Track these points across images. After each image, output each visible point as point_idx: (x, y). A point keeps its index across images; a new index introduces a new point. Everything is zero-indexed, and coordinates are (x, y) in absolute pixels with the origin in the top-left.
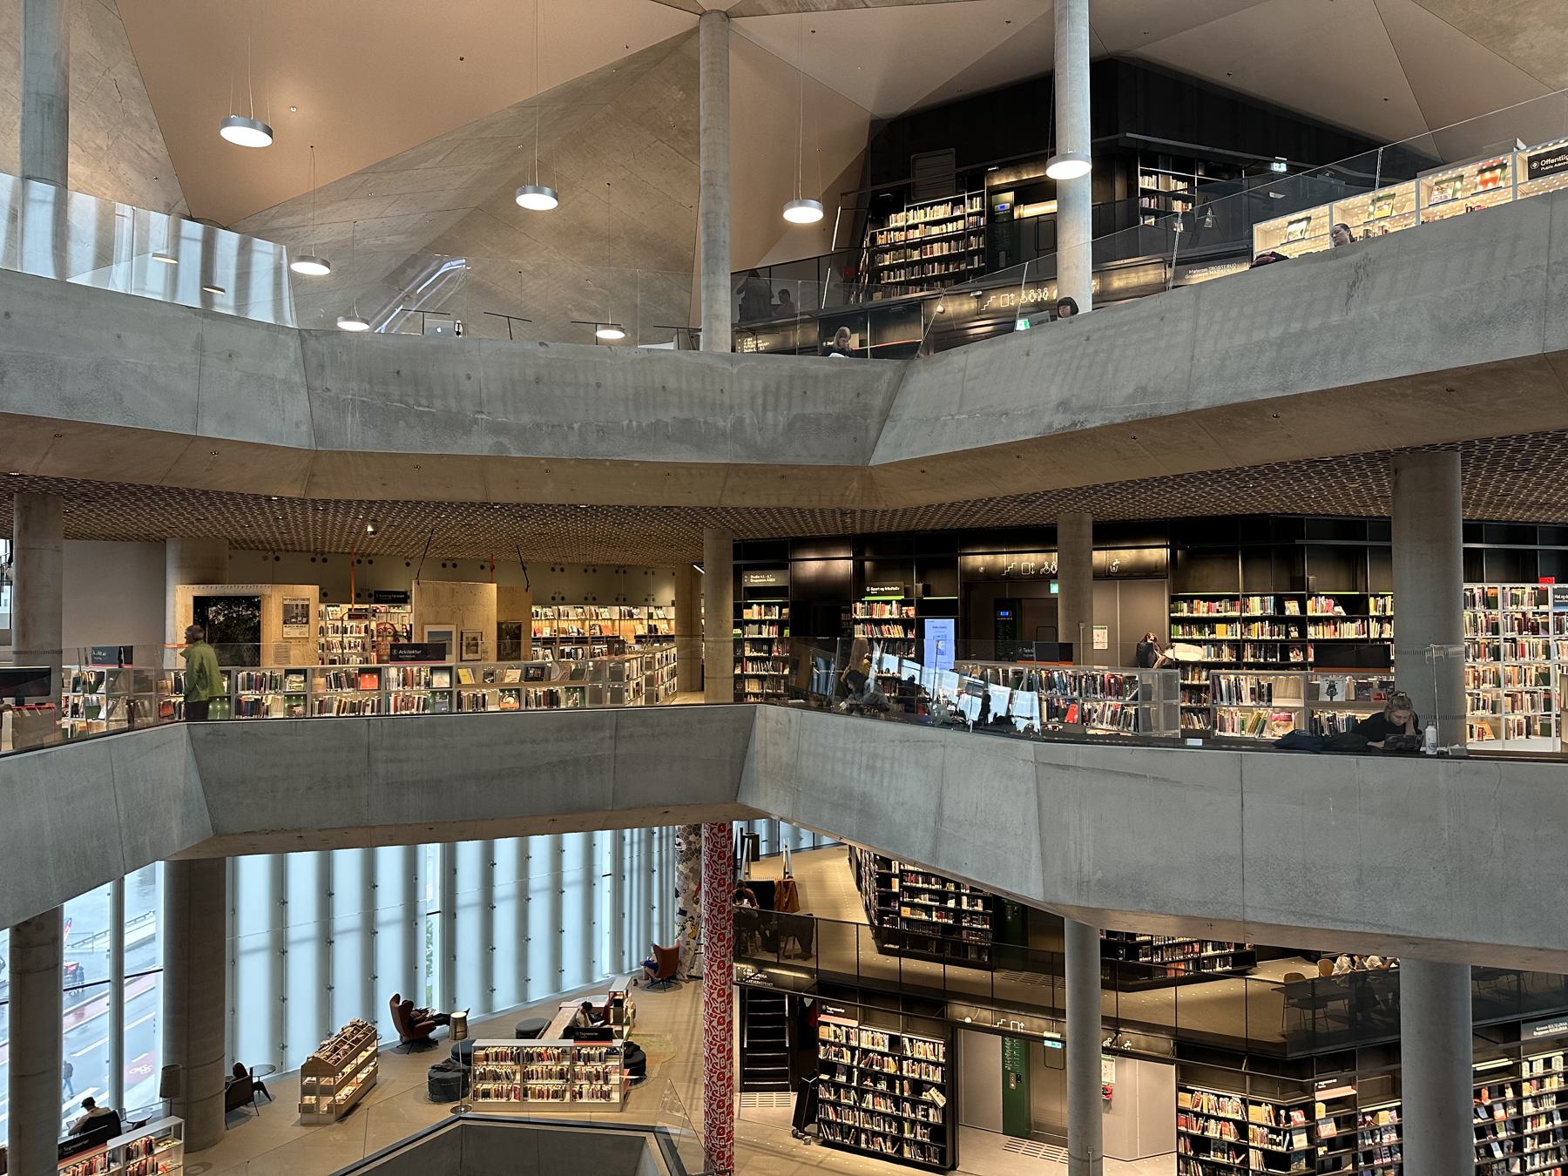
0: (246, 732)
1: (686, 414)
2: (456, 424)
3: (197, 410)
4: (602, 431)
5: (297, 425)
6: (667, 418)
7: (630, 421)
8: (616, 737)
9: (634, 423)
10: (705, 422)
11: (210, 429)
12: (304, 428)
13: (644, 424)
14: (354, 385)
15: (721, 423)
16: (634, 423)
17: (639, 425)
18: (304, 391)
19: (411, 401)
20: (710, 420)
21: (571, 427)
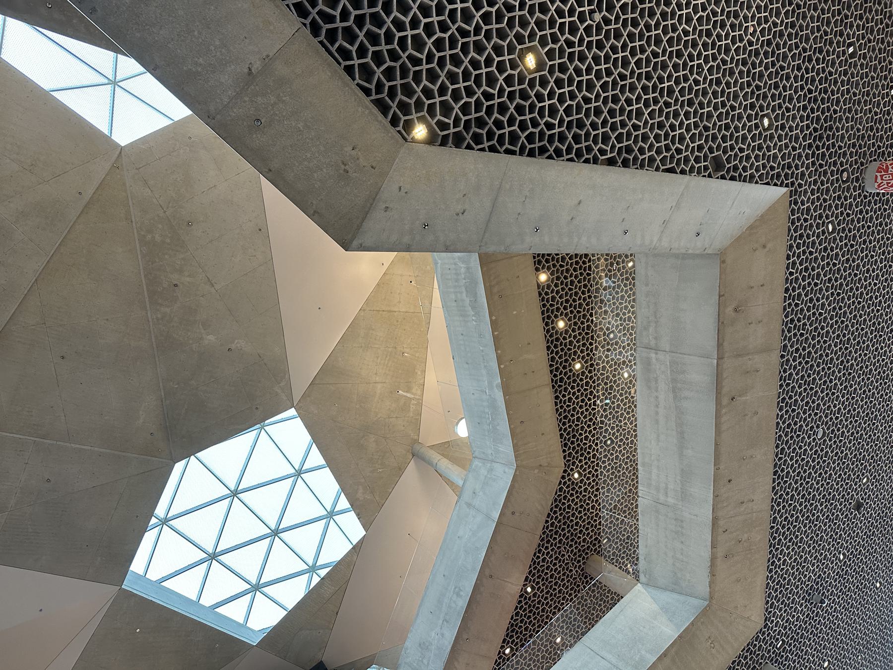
0: (645, 559)
1: (463, 289)
2: (493, 404)
3: (488, 517)
4: (481, 335)
5: (505, 472)
6: (467, 301)
7: (473, 320)
8: (657, 350)
9: (474, 318)
10: (465, 279)
11: (496, 515)
12: (507, 470)
13: (473, 313)
14: (488, 443)
15: (463, 270)
16: (474, 318)
17: (473, 316)
18: (494, 464)
19: (488, 422)
20: (463, 276)
21: (482, 351)
